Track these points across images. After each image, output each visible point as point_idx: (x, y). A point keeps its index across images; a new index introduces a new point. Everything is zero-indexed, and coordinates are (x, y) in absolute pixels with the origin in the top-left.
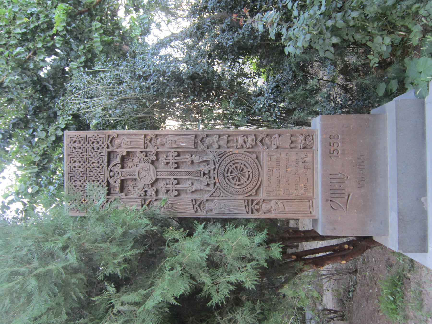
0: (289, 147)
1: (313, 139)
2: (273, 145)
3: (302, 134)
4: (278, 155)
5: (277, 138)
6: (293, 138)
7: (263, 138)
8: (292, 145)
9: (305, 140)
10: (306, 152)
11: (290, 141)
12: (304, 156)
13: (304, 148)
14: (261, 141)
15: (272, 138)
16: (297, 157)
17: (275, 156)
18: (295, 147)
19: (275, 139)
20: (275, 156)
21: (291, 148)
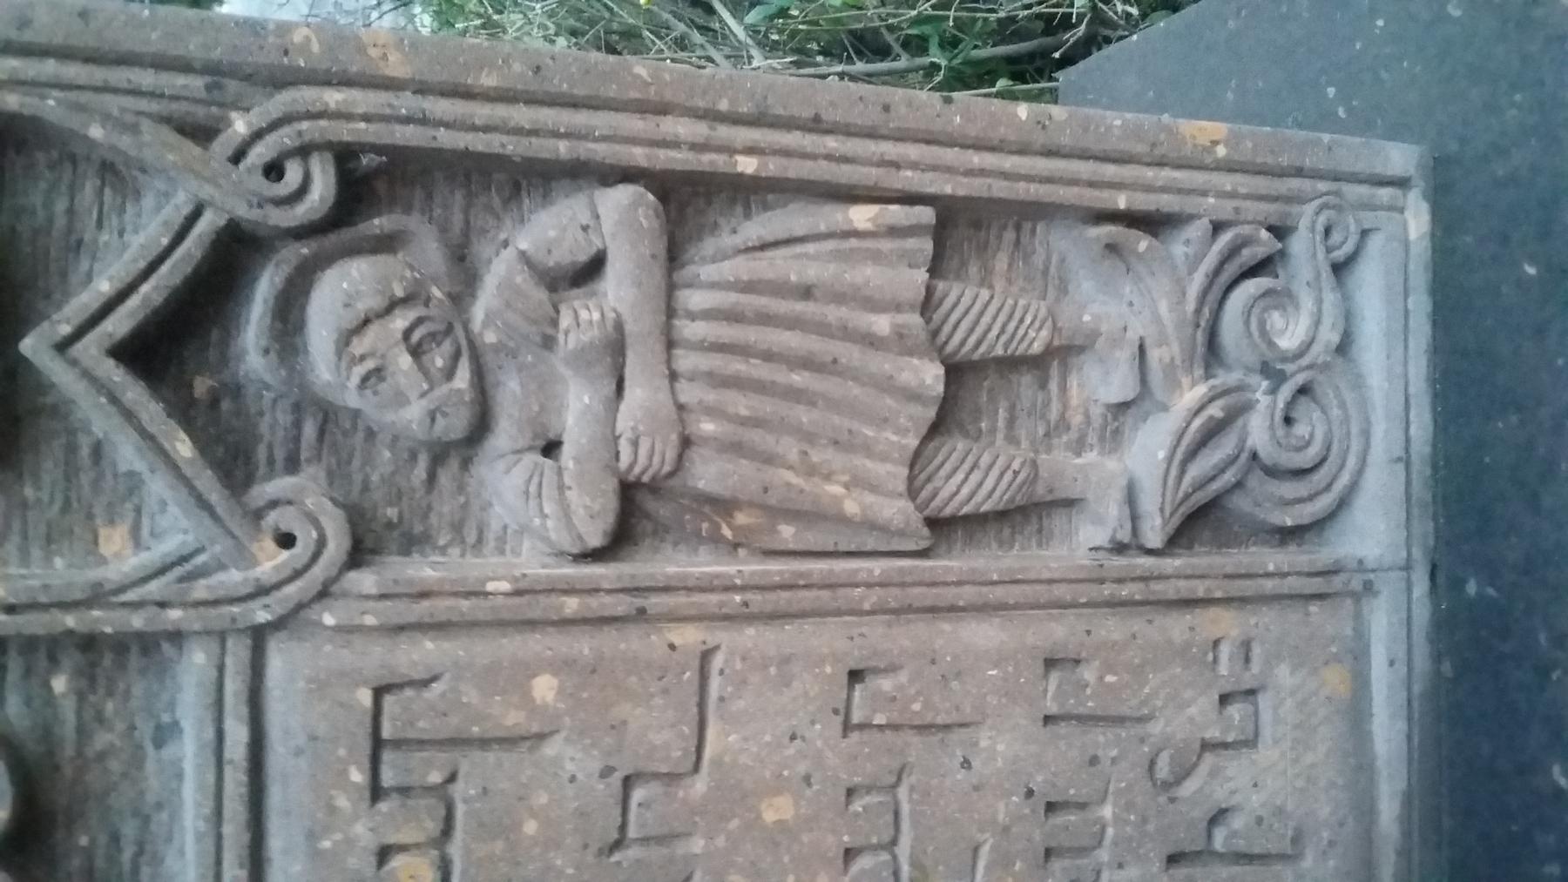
0: (896, 510)
1: (1343, 348)
2: (504, 479)
3: (1153, 223)
4: (656, 729)
5: (620, 292)
6: (992, 308)
7: (234, 253)
8: (973, 476)
9: (1212, 352)
10: (1227, 624)
11: (931, 375)
12: (1197, 715)
13: (1200, 521)
14: (174, 344)
15: (500, 274)
16: (1070, 745)
17: (571, 758)
18: (1027, 513)
19: (582, 318)
20: (571, 758)
21: (944, 527)
